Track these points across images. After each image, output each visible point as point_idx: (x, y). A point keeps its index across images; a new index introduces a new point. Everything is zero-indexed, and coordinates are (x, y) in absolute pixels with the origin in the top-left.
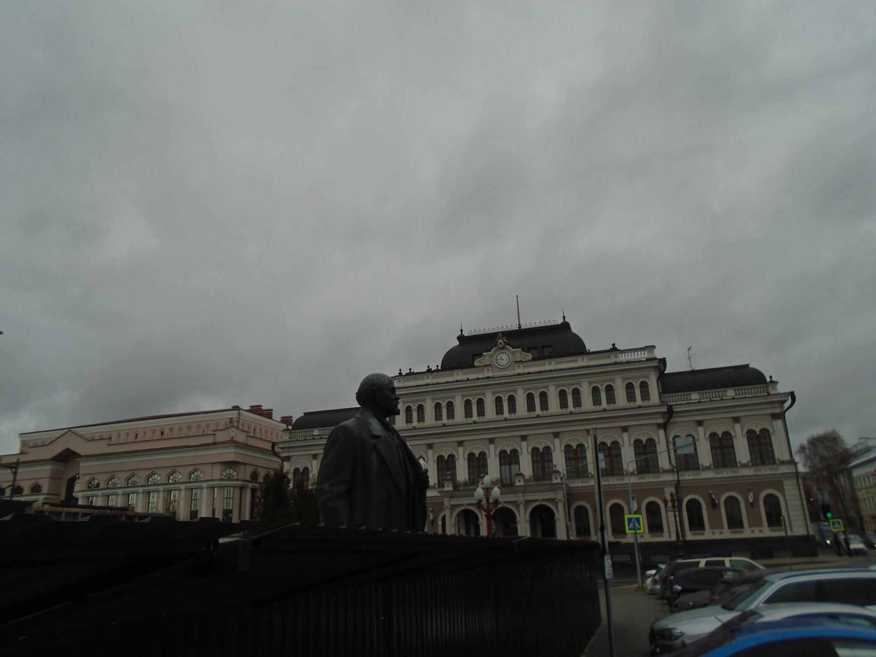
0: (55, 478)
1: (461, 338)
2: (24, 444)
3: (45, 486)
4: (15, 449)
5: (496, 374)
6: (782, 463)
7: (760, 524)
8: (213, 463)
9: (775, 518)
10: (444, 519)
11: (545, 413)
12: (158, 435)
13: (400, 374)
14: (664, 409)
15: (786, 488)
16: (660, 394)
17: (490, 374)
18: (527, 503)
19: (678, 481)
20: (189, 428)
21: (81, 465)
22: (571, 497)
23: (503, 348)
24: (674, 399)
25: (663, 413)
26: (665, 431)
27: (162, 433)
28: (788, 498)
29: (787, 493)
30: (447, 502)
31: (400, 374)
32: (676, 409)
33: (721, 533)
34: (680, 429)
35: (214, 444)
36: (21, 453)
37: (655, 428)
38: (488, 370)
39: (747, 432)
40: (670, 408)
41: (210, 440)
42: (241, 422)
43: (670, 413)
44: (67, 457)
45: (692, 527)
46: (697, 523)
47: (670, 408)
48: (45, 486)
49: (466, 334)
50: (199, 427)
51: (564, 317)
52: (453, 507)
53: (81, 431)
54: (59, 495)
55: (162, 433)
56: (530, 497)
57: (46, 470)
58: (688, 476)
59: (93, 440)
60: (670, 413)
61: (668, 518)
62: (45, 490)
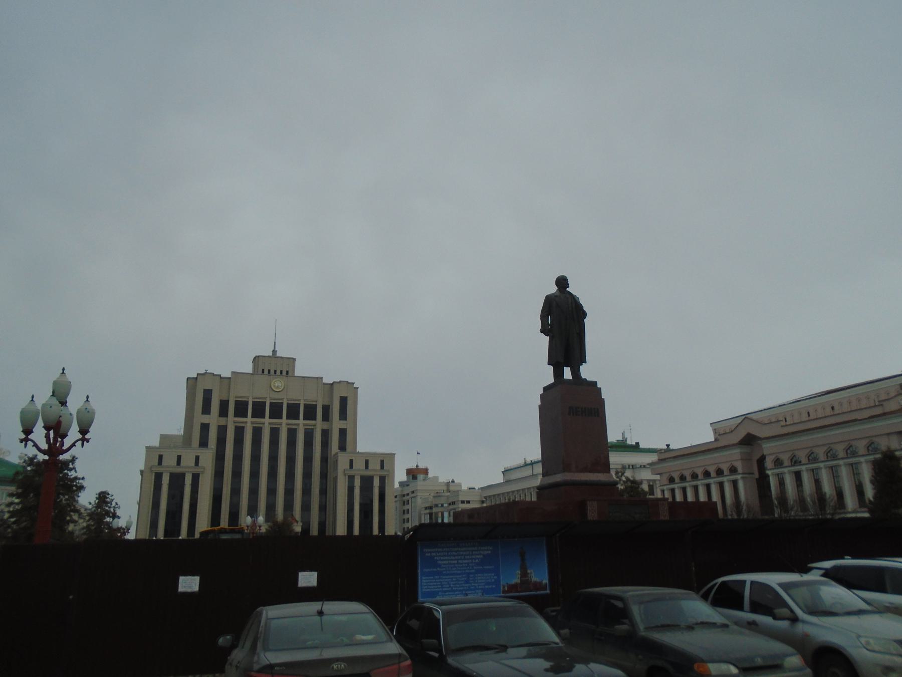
0: (746, 459)
2: (715, 431)
3: (739, 465)
4: (711, 438)
8: (888, 434)
12: (828, 411)
20: (859, 400)
21: (764, 446)
27: (833, 408)
35: (884, 414)
36: (716, 440)
41: (879, 411)
44: (749, 440)
48: (739, 465)
50: (868, 398)
53: (754, 417)
54: (753, 474)
55: (833, 408)
57: (736, 453)
59: (771, 423)
62: (740, 470)
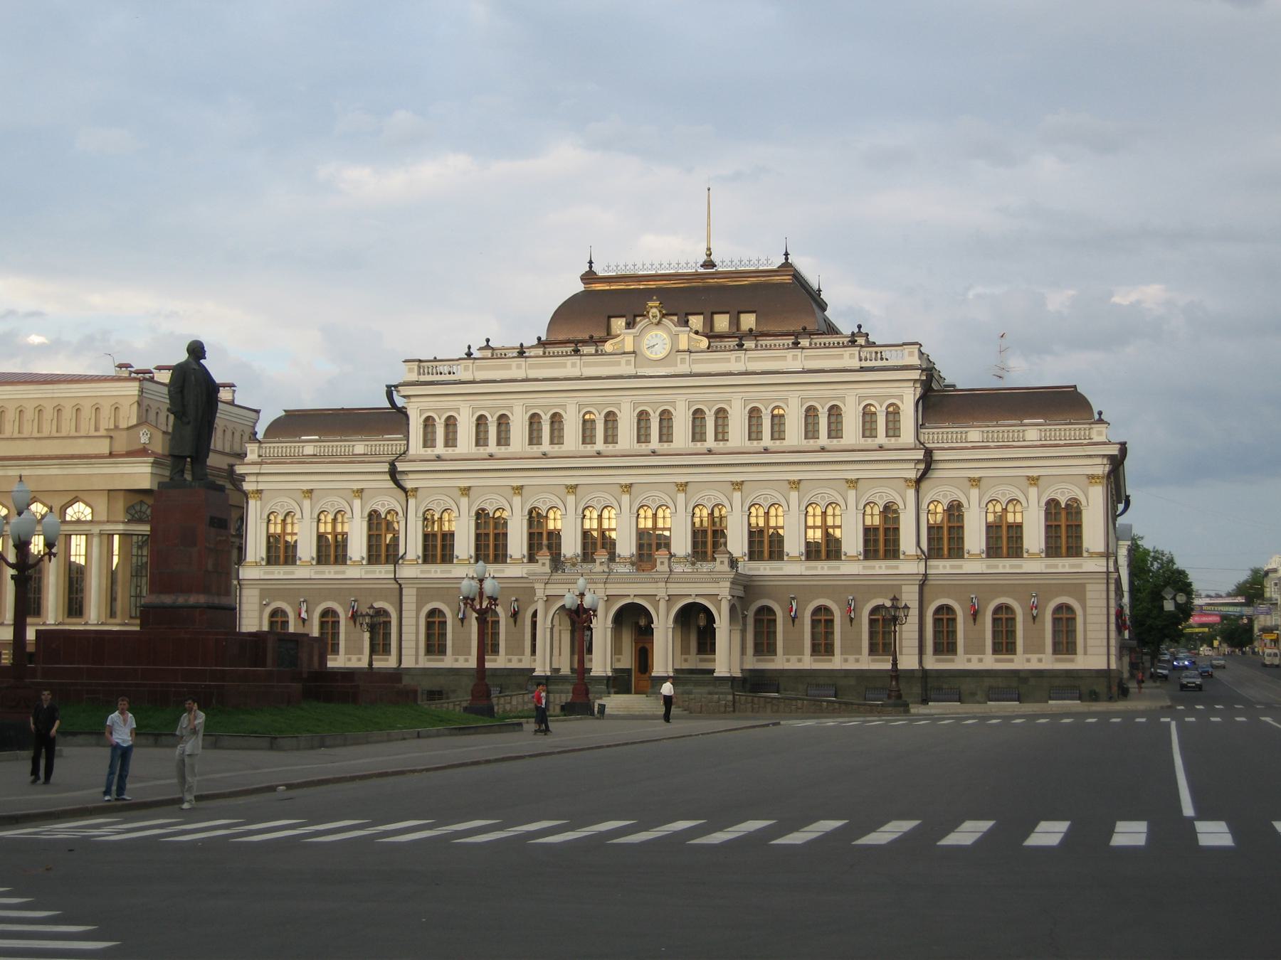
1: (589, 277)
5: (641, 372)
6: (1092, 555)
7: (1040, 650)
9: (1065, 641)
10: (535, 614)
11: (721, 446)
13: (469, 354)
14: (920, 455)
15: (1089, 595)
16: (919, 427)
17: (630, 370)
18: (671, 598)
19: (926, 575)
22: (746, 590)
23: (659, 323)
24: (937, 436)
25: (919, 461)
26: (917, 491)
28: (1089, 611)
29: (1089, 603)
30: (540, 592)
31: (469, 354)
32: (937, 455)
33: (981, 660)
34: (939, 494)
37: (903, 484)
38: (628, 363)
39: (1048, 503)
40: (929, 453)
42: (146, 402)
43: (929, 461)
45: (937, 650)
46: (945, 645)
47: (929, 453)
49: (600, 270)
51: (786, 254)
52: (549, 599)
56: (675, 589)
58: (942, 567)
60: (929, 461)
61: (908, 633)
